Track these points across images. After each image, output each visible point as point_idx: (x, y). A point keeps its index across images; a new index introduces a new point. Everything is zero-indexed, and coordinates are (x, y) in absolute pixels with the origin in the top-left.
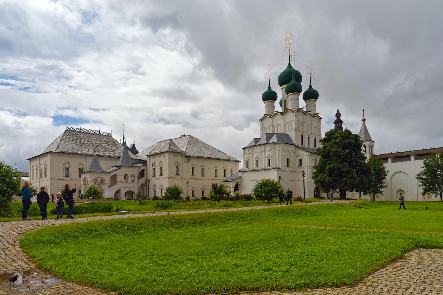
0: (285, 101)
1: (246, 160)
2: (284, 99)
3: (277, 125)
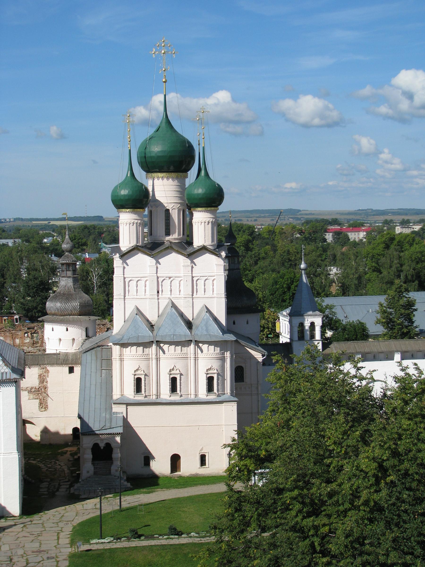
3: (170, 278)
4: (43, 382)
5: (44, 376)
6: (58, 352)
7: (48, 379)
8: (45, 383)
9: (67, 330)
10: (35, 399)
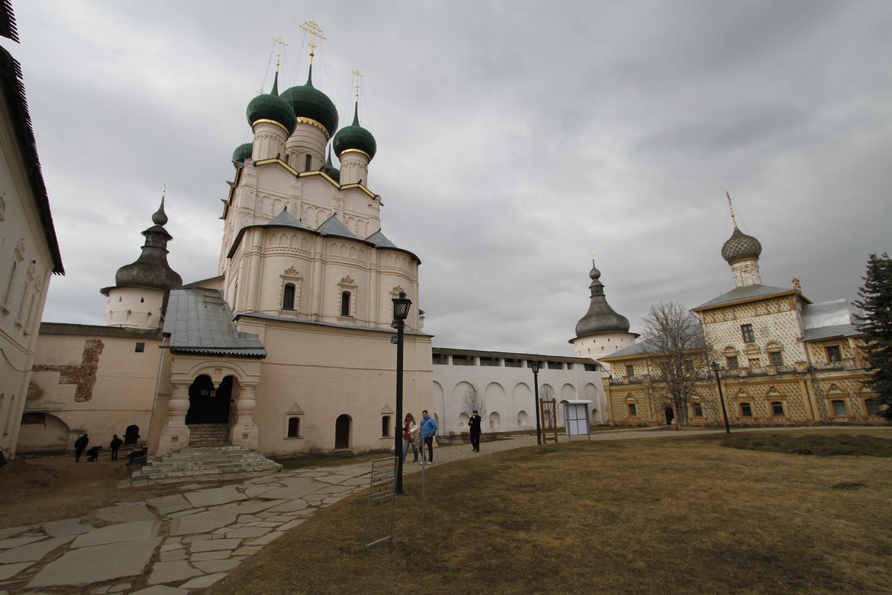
0: (309, 157)
1: (284, 277)
2: (306, 150)
3: (317, 207)
4: (91, 361)
5: (95, 352)
6: (122, 326)
7: (100, 357)
8: (93, 362)
9: (142, 301)
10: (71, 383)
